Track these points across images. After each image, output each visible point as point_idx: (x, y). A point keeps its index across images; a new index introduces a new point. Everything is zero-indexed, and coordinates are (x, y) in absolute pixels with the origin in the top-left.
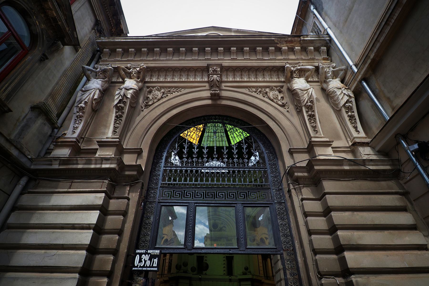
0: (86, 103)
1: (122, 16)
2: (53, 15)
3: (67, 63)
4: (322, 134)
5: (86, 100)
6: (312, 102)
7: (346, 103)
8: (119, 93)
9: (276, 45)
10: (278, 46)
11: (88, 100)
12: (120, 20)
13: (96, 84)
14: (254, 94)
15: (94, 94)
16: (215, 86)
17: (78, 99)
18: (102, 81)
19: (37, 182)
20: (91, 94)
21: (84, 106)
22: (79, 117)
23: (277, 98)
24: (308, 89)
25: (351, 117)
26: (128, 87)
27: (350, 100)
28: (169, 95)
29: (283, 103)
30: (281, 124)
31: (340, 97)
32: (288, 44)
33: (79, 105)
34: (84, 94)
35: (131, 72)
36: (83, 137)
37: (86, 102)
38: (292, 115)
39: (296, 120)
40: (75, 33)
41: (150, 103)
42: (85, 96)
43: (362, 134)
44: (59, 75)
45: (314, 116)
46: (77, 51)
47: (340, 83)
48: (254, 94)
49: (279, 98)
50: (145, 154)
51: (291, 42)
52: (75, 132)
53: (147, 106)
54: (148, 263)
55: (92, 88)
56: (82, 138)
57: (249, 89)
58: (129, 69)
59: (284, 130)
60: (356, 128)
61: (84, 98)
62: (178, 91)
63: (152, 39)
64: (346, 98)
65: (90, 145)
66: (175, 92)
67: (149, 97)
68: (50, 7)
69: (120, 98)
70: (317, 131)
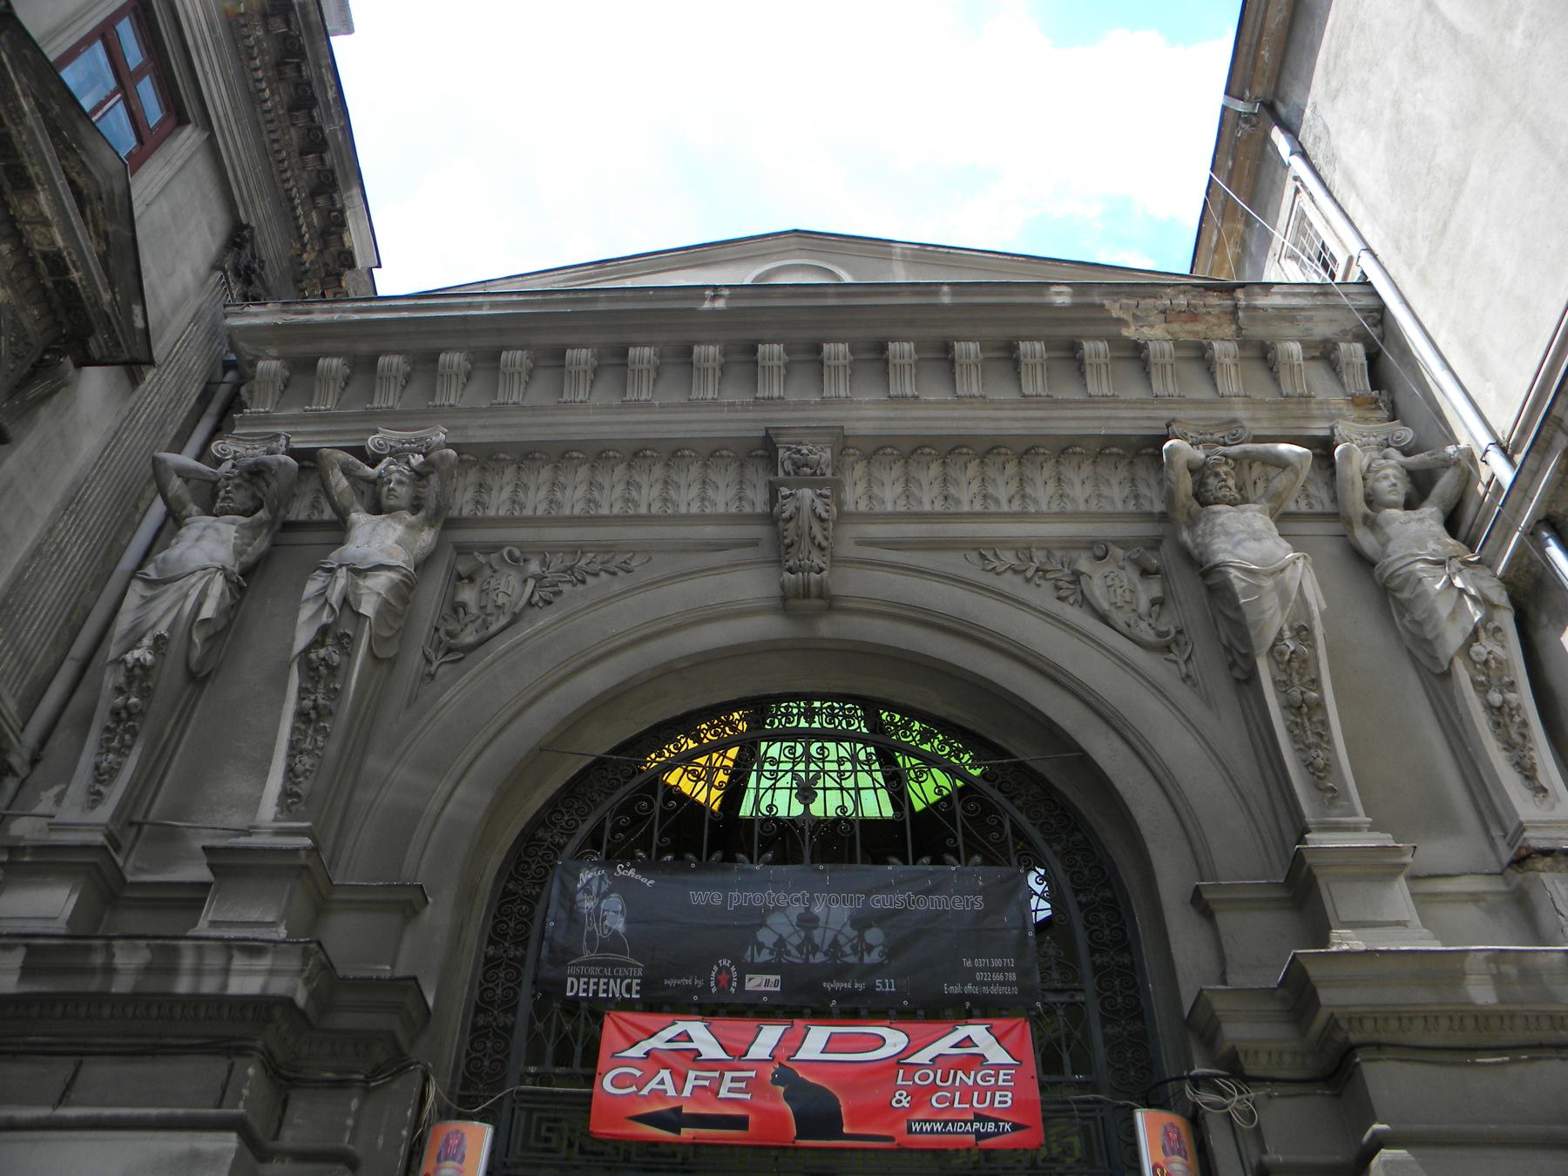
0: (159, 644)
1: (356, 191)
2: (53, 243)
3: (89, 445)
4: (1359, 808)
5: (162, 629)
6: (1303, 632)
7: (1474, 636)
8: (322, 593)
9: (1112, 329)
10: (1125, 332)
11: (171, 629)
12: (342, 212)
13: (211, 544)
14: (1009, 583)
15: (203, 595)
16: (806, 543)
17: (124, 622)
18: (242, 526)
20: (186, 596)
21: (149, 657)
22: (124, 715)
24: (1283, 570)
25: (1500, 715)
26: (365, 557)
27: (1490, 626)
28: (566, 588)
29: (1160, 634)
30: (1151, 749)
31: (1444, 609)
32: (1175, 327)
33: (129, 657)
34: (153, 599)
35: (380, 476)
36: (138, 817)
37: (161, 637)
38: (1208, 701)
39: (1228, 730)
40: (137, 309)
41: (469, 638)
42: (161, 606)
44: (45, 509)
46: (135, 380)
47: (1439, 529)
48: (1009, 583)
49: (1143, 605)
50: (438, 915)
51: (1192, 315)
52: (99, 793)
53: (457, 653)
55: (192, 566)
56: (131, 824)
57: (983, 557)
58: (374, 461)
59: (1166, 783)
61: (153, 617)
62: (611, 567)
63: (493, 305)
66: (596, 575)
67: (464, 605)
68: (41, 214)
69: (325, 618)
70: (1333, 790)
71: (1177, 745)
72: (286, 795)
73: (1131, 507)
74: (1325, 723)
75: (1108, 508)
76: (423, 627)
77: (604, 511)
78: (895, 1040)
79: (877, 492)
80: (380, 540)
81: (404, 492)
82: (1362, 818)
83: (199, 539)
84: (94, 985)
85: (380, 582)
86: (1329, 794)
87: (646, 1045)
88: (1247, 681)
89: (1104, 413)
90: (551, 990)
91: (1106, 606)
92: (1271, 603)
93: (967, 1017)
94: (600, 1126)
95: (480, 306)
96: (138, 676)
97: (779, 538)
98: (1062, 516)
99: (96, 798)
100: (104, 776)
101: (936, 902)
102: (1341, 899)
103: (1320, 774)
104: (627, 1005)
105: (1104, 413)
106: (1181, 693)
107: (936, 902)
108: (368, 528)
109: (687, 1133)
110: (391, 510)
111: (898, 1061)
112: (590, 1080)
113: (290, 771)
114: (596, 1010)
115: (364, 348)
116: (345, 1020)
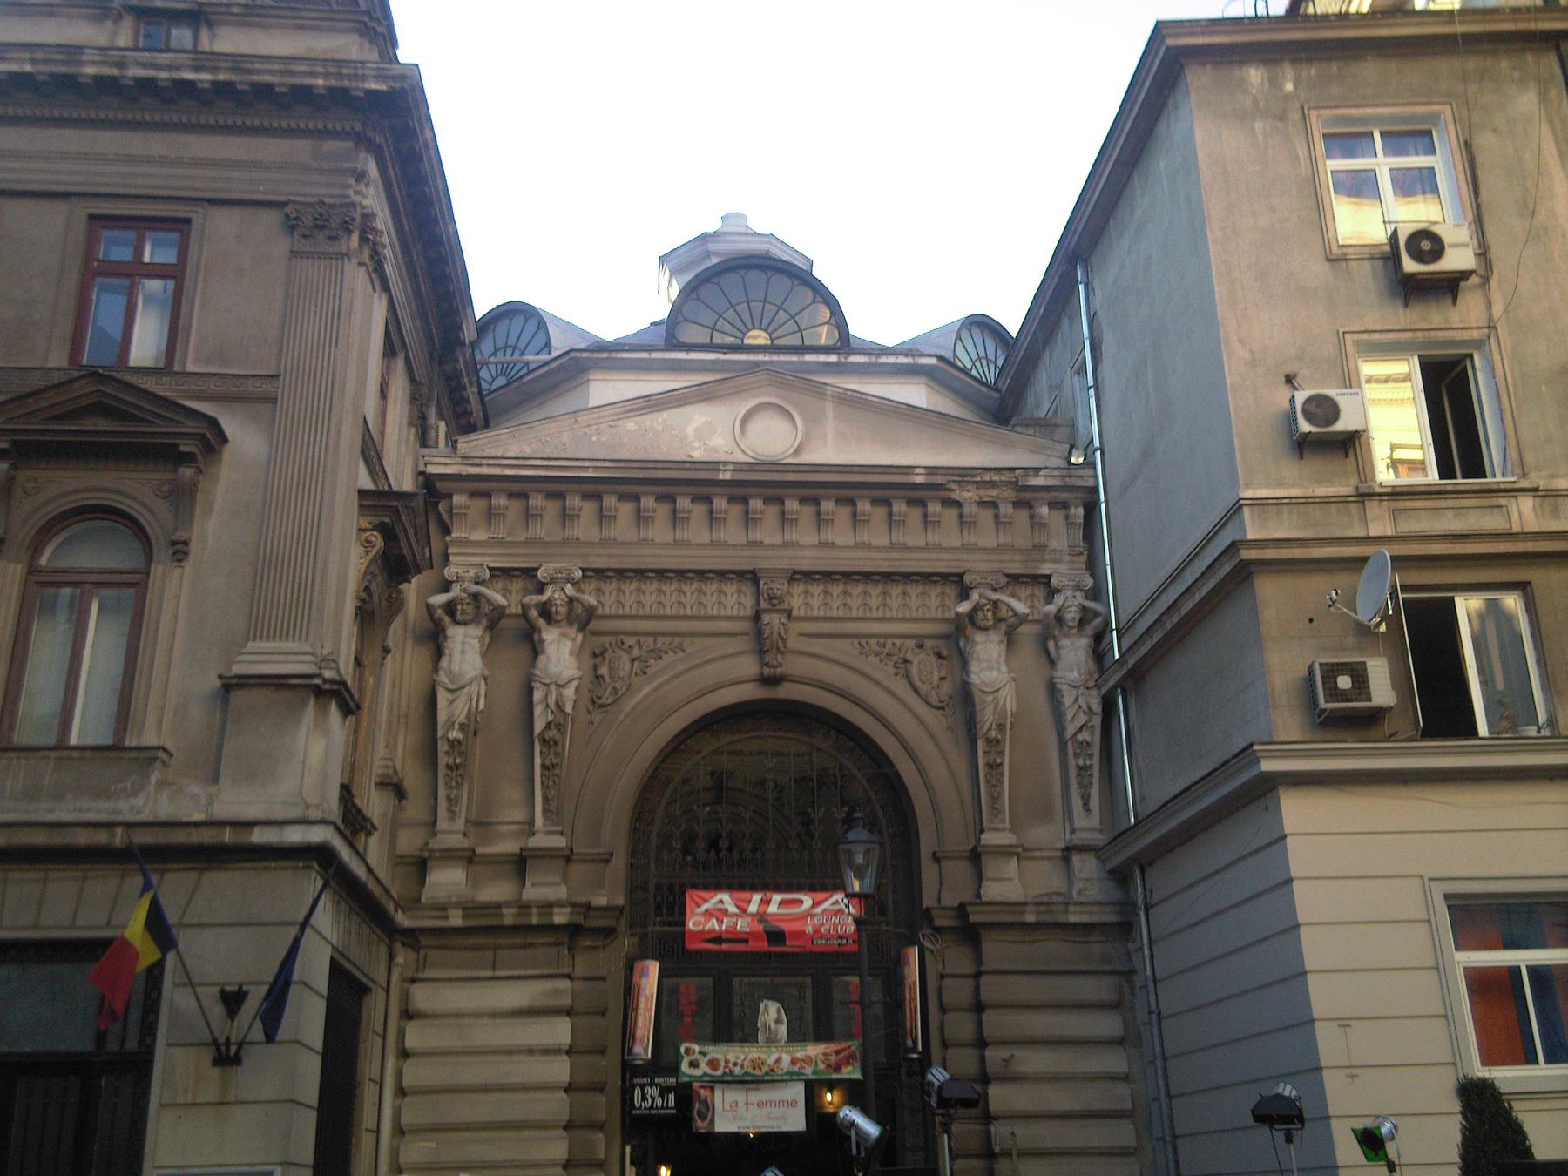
0: (462, 727)
5: (462, 718)
6: (1001, 727)
9: (943, 494)
11: (468, 717)
14: (871, 665)
17: (442, 716)
19: (422, 952)
28: (652, 662)
32: (982, 492)
43: (1095, 821)
45: (1001, 764)
50: (620, 862)
54: (659, 1101)
58: (541, 588)
60: (1086, 804)
64: (1082, 719)
69: (550, 718)
71: (939, 773)
72: (545, 811)
73: (939, 615)
74: (1002, 774)
75: (927, 615)
77: (668, 612)
78: (807, 900)
80: (561, 654)
81: (562, 610)
82: (1007, 825)
83: (463, 652)
85: (569, 692)
86: (996, 811)
87: (705, 906)
88: (973, 742)
89: (934, 556)
91: (918, 683)
92: (989, 711)
94: (692, 946)
95: (586, 468)
96: (453, 743)
97: (762, 644)
99: (453, 816)
102: (991, 866)
103: (995, 799)
105: (934, 556)
108: (554, 646)
109: (725, 946)
113: (546, 799)
115: (516, 487)
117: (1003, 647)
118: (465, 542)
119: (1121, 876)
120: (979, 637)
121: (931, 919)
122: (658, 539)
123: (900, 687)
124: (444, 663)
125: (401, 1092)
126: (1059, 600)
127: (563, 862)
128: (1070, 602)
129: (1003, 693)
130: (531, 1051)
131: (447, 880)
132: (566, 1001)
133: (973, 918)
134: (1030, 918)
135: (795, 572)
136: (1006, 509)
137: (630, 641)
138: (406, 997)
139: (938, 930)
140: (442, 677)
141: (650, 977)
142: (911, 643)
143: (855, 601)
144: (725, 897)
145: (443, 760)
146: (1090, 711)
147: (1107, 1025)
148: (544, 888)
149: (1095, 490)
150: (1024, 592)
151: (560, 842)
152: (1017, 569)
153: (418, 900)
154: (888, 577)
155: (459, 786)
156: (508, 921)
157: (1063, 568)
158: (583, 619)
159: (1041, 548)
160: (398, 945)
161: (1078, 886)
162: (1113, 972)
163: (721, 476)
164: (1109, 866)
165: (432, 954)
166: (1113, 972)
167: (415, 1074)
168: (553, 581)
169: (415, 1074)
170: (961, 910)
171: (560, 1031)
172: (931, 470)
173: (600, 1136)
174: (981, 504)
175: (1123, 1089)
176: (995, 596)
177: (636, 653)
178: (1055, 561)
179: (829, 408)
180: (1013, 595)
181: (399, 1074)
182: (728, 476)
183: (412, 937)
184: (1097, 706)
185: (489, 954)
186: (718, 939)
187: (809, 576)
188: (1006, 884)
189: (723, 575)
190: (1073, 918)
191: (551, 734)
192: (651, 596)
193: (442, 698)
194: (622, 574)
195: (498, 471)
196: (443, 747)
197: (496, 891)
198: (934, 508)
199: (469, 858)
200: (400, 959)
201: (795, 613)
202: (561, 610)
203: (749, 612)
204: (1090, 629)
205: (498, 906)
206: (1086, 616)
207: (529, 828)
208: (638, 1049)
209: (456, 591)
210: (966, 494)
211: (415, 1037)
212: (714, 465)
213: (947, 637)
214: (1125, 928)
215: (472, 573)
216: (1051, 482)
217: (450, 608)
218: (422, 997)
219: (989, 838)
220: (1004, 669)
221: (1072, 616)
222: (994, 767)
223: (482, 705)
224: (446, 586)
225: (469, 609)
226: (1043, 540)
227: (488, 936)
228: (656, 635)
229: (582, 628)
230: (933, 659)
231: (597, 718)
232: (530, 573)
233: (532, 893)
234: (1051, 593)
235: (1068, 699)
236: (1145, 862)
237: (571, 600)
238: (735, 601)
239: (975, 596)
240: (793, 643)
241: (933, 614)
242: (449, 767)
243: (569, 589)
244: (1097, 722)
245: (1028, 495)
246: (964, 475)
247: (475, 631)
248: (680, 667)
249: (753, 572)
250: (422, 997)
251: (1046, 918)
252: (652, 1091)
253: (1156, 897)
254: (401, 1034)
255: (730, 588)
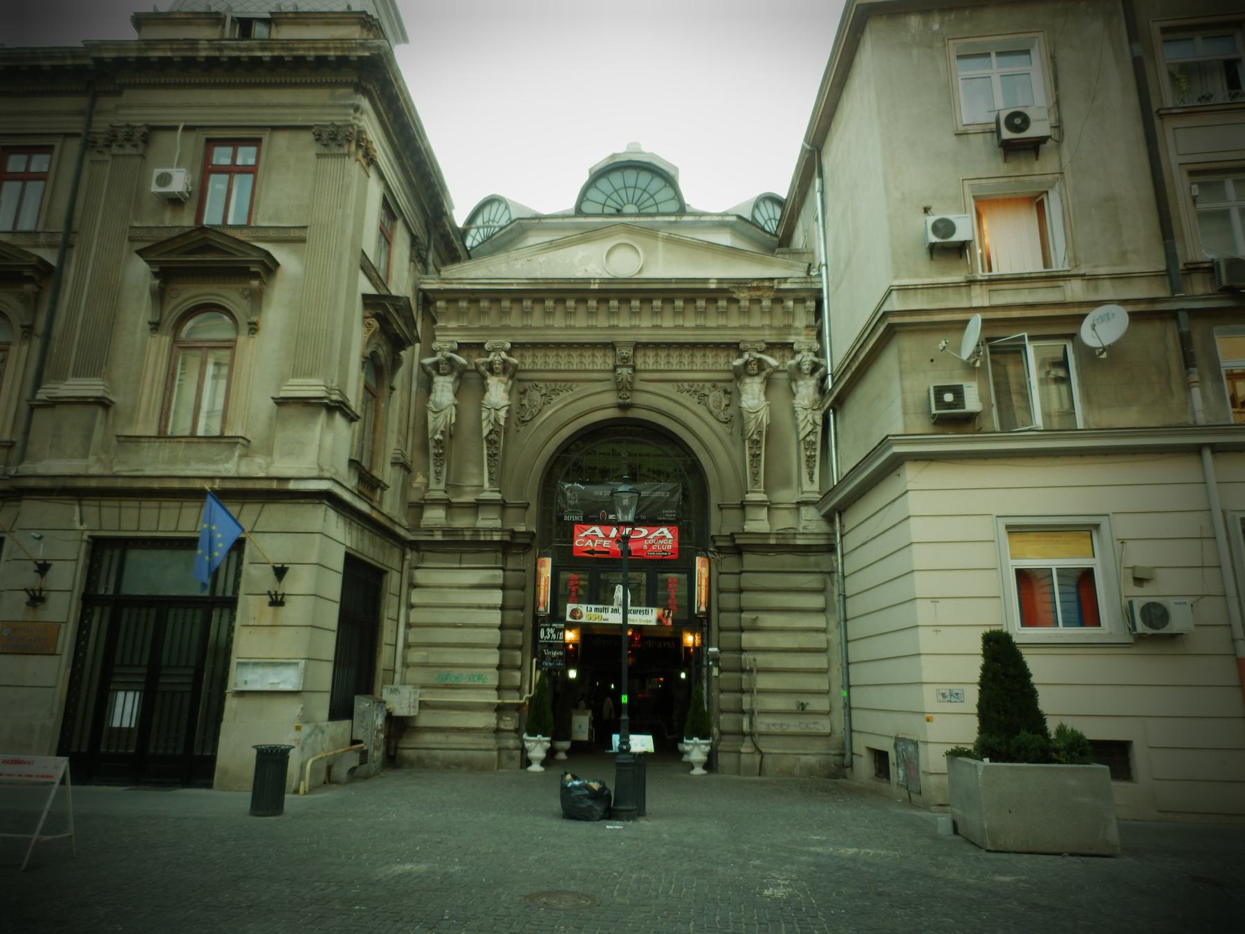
0: (442, 433)
6: (760, 433)
17: (431, 427)
23: (719, 407)
25: (810, 458)
39: (736, 453)
41: (527, 418)
43: (816, 487)
50: (533, 508)
51: (758, 288)
58: (488, 353)
60: (811, 475)
64: (809, 428)
65: (458, 496)
71: (722, 458)
72: (490, 479)
76: (514, 413)
78: (645, 532)
79: (647, 361)
80: (497, 393)
81: (500, 367)
84: (460, 538)
85: (502, 414)
86: (756, 482)
90: (561, 519)
93: (662, 526)
94: (575, 554)
96: (438, 442)
98: (704, 371)
100: (438, 473)
101: (657, 494)
104: (579, 523)
106: (727, 440)
107: (657, 494)
110: (498, 374)
111: (645, 538)
112: (572, 542)
113: (490, 473)
114: (573, 523)
116: (519, 541)
117: (763, 387)
118: (445, 329)
119: (829, 518)
120: (748, 380)
121: (714, 542)
122: (559, 326)
123: (701, 410)
124: (432, 397)
125: (409, 626)
126: (798, 357)
127: (498, 508)
128: (807, 359)
129: (762, 413)
130: (479, 607)
131: (434, 516)
132: (500, 581)
133: (738, 542)
134: (773, 541)
135: (637, 343)
136: (766, 303)
137: (541, 385)
138: (411, 577)
139: (718, 548)
140: (431, 405)
141: (546, 569)
142: (708, 385)
143: (674, 361)
144: (596, 529)
145: (432, 451)
146: (815, 423)
147: (817, 601)
148: (489, 521)
149: (821, 290)
150: (778, 353)
151: (497, 496)
152: (773, 340)
153: (419, 526)
154: (693, 346)
155: (441, 465)
156: (467, 538)
157: (802, 338)
158: (509, 371)
159: (789, 327)
160: (408, 550)
161: (804, 523)
162: (821, 572)
163: (592, 287)
164: (823, 512)
165: (427, 555)
166: (821, 572)
167: (416, 616)
168: (494, 350)
169: (416, 616)
170: (732, 536)
171: (496, 597)
172: (720, 281)
173: (519, 654)
174: (752, 301)
175: (822, 637)
176: (759, 356)
177: (544, 391)
178: (797, 334)
179: (660, 245)
180: (771, 356)
181: (407, 617)
182: (596, 287)
183: (415, 546)
184: (819, 421)
185: (458, 556)
186: (592, 552)
187: (645, 345)
188: (758, 523)
189: (593, 346)
190: (799, 542)
191: (493, 436)
192: (551, 360)
193: (431, 417)
194: (535, 346)
195: (462, 287)
196: (432, 444)
197: (462, 522)
198: (722, 303)
199: (448, 505)
200: (408, 557)
201: (638, 367)
202: (498, 366)
203: (611, 367)
204: (817, 375)
205: (462, 529)
206: (815, 367)
207: (480, 487)
208: (541, 609)
209: (439, 356)
210: (742, 295)
211: (416, 597)
212: (587, 281)
213: (730, 381)
214: (830, 549)
215: (448, 346)
216: (795, 286)
217: (436, 365)
218: (420, 576)
219: (751, 497)
220: (763, 398)
221: (806, 367)
222: (755, 457)
223: (453, 420)
224: (434, 353)
225: (447, 367)
226: (790, 322)
227: (457, 546)
228: (556, 381)
229: (511, 377)
230: (722, 393)
231: (522, 429)
232: (480, 346)
233: (481, 523)
234: (795, 353)
235: (801, 417)
236: (841, 509)
237: (504, 361)
238: (602, 361)
239: (746, 356)
240: (639, 385)
241: (722, 368)
242: (436, 455)
243: (504, 355)
244: (819, 429)
245: (780, 295)
246: (741, 283)
247: (450, 379)
248: (570, 400)
249: (612, 343)
250: (420, 576)
251: (782, 542)
252: (552, 631)
253: (847, 529)
254: (409, 595)
255: (599, 354)
